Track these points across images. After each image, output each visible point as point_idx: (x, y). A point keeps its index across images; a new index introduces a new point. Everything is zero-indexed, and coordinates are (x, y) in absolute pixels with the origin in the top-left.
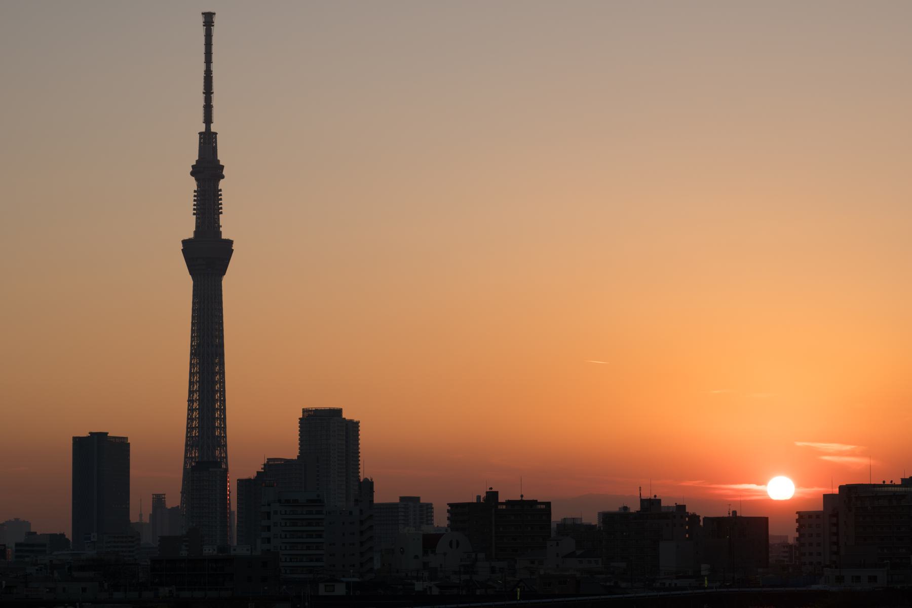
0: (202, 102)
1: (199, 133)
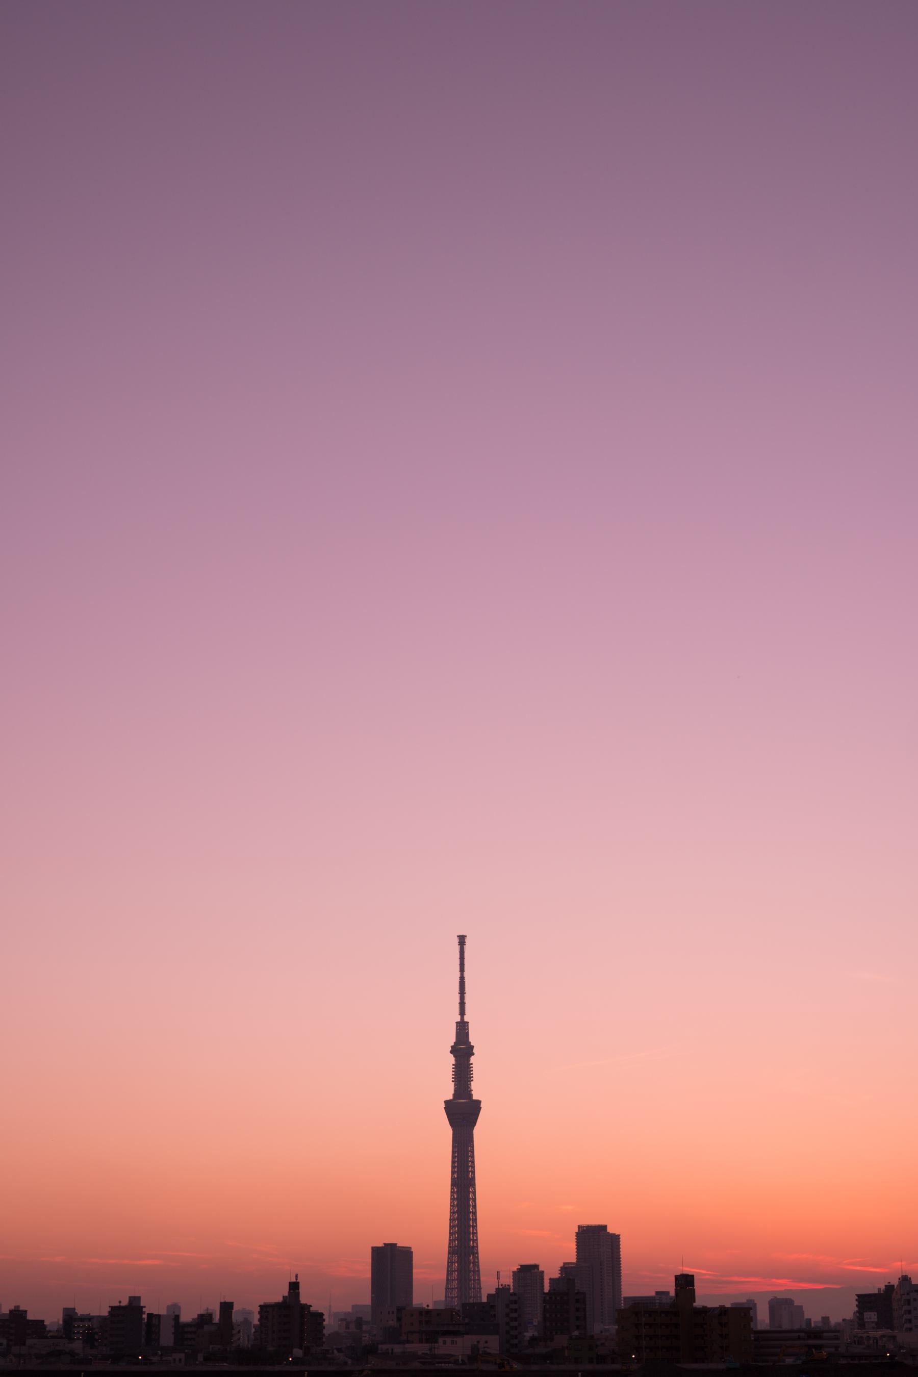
0: (458, 1000)
1: (456, 1023)
